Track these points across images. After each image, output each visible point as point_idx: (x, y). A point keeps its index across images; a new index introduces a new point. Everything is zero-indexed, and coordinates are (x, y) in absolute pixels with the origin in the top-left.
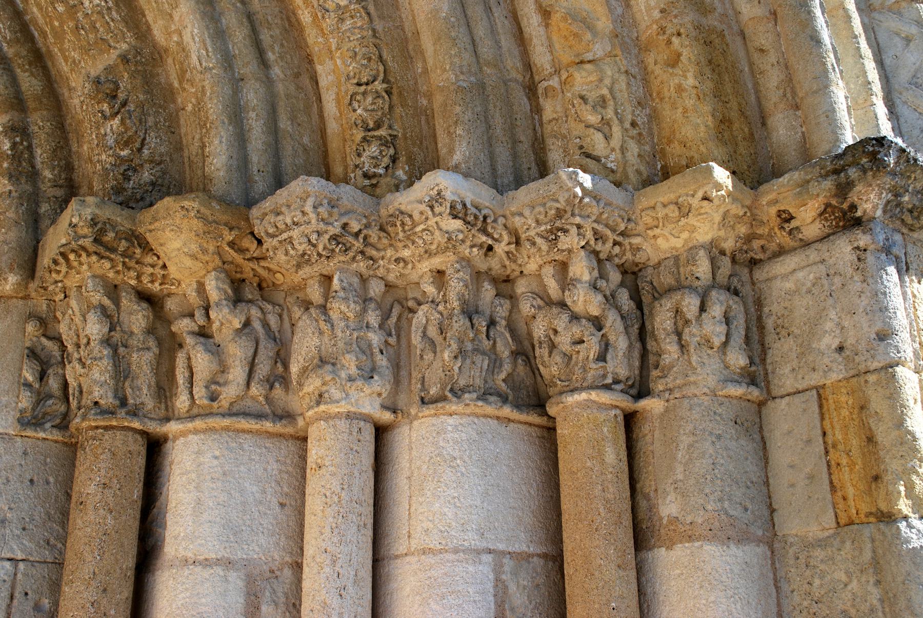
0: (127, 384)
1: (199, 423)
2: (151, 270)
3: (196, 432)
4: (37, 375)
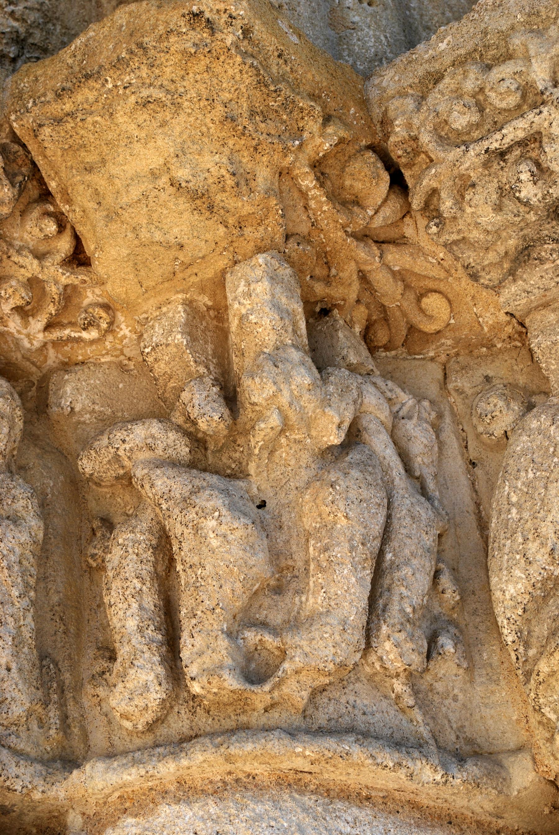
1: (201, 762)
2: (32, 267)
3: (186, 791)
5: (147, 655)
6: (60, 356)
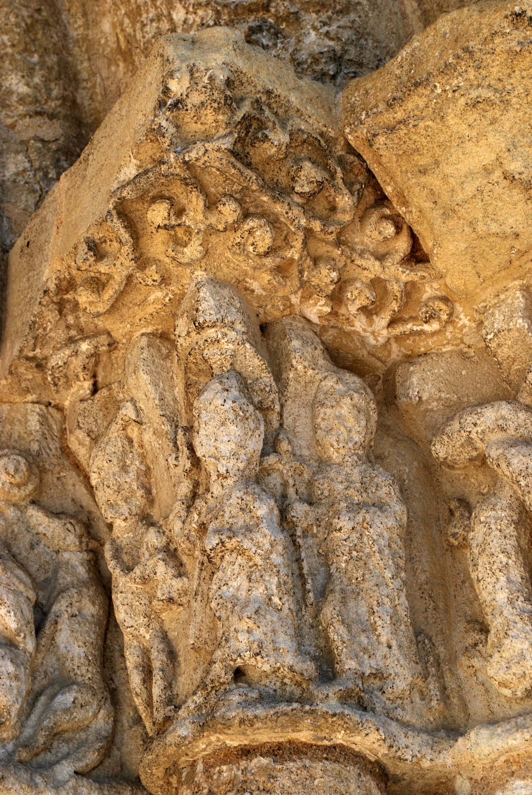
0: (329, 611)
2: (374, 268)
4: (29, 614)
5: (520, 625)
6: (403, 349)
